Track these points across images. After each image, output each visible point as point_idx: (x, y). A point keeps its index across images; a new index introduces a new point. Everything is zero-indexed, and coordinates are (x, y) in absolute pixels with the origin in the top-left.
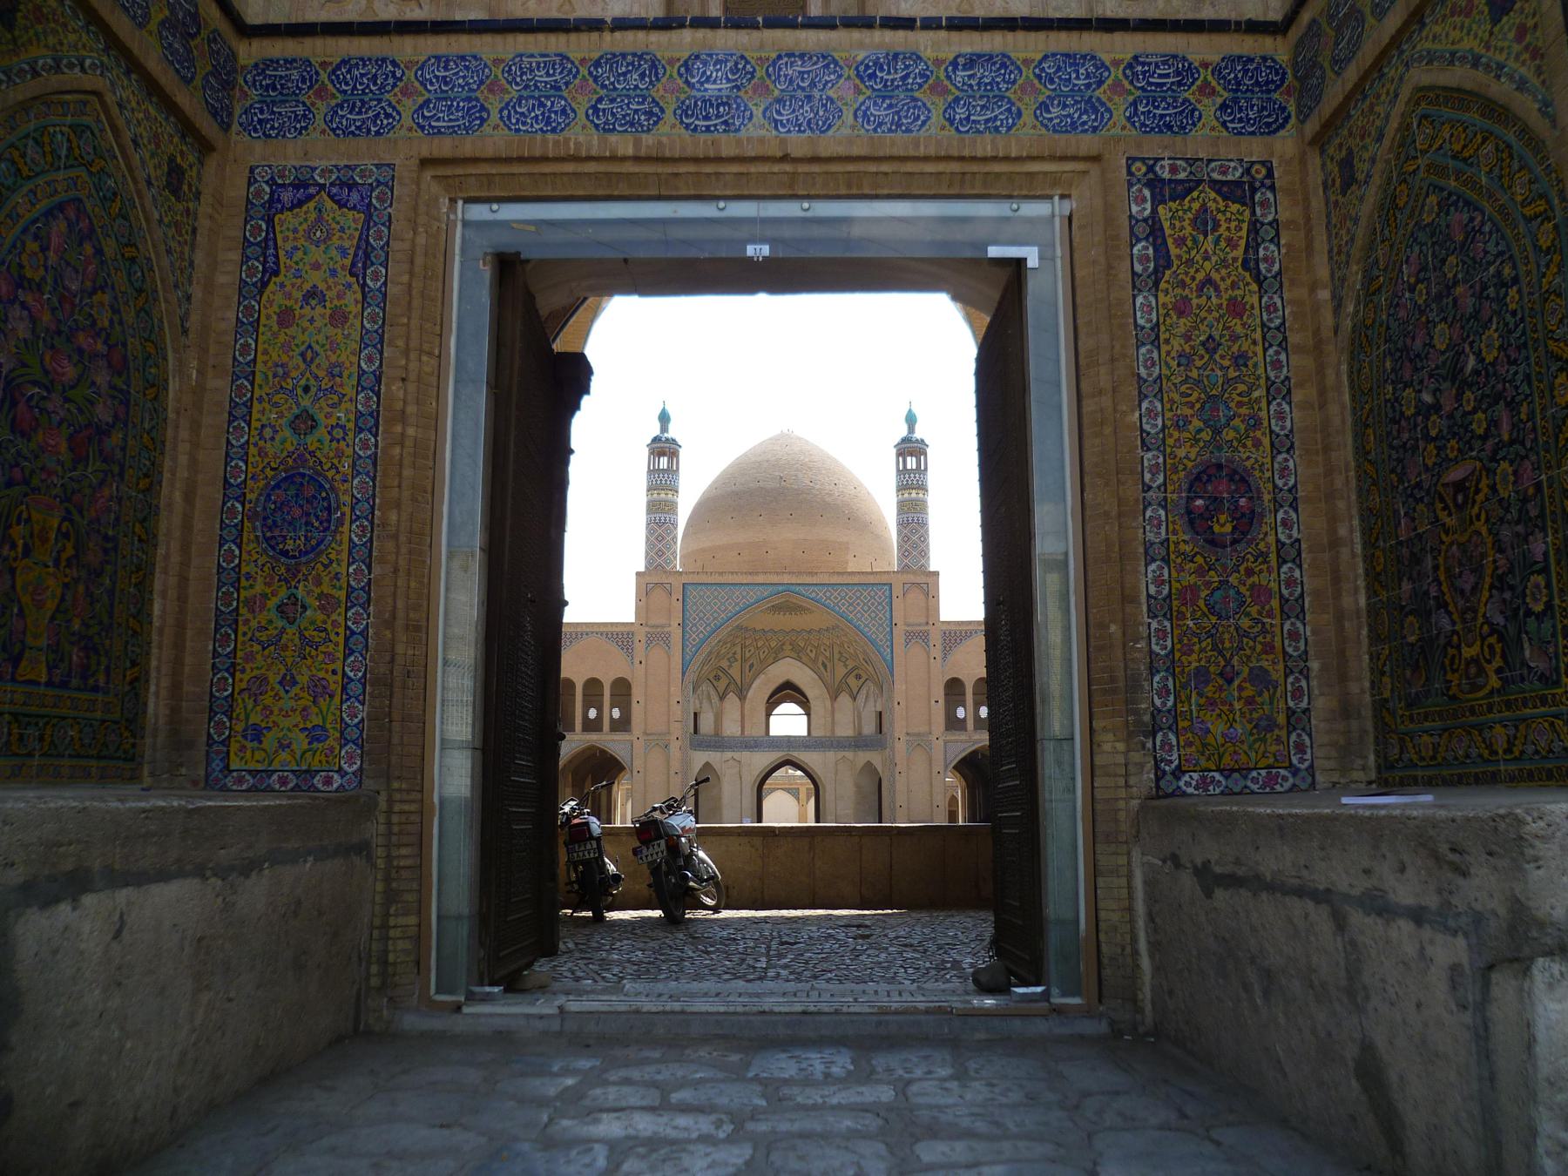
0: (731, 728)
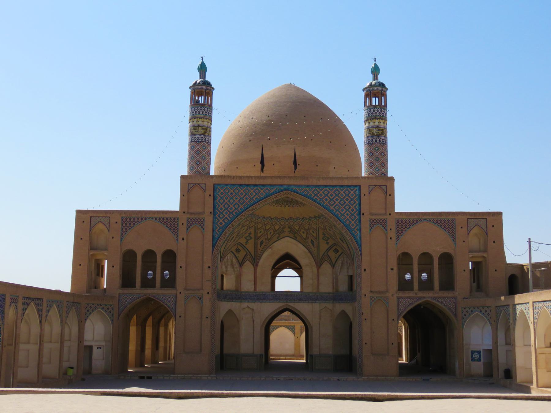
0: (247, 286)
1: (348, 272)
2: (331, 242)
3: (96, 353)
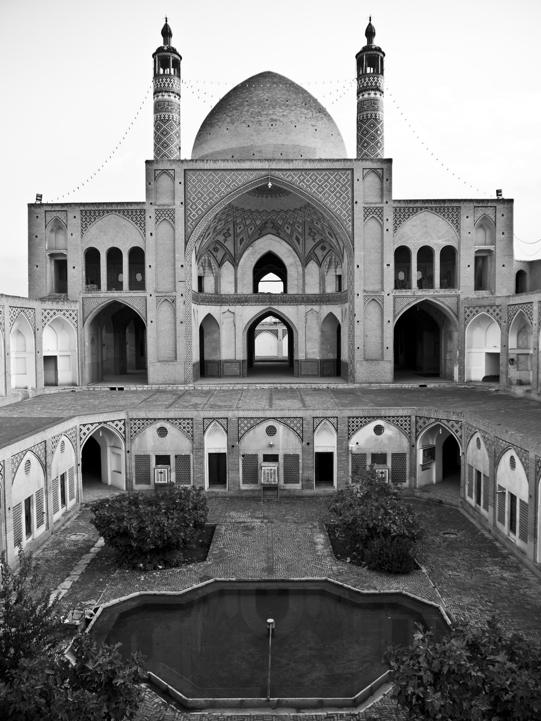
0: (227, 288)
1: (336, 272)
2: (318, 238)
3: (60, 362)
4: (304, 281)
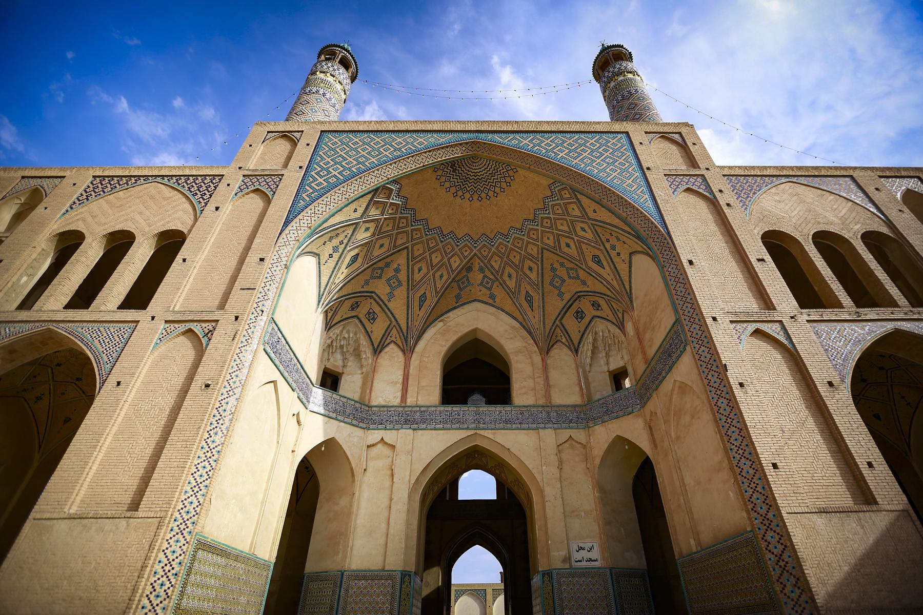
0: (386, 393)
4: (547, 378)
